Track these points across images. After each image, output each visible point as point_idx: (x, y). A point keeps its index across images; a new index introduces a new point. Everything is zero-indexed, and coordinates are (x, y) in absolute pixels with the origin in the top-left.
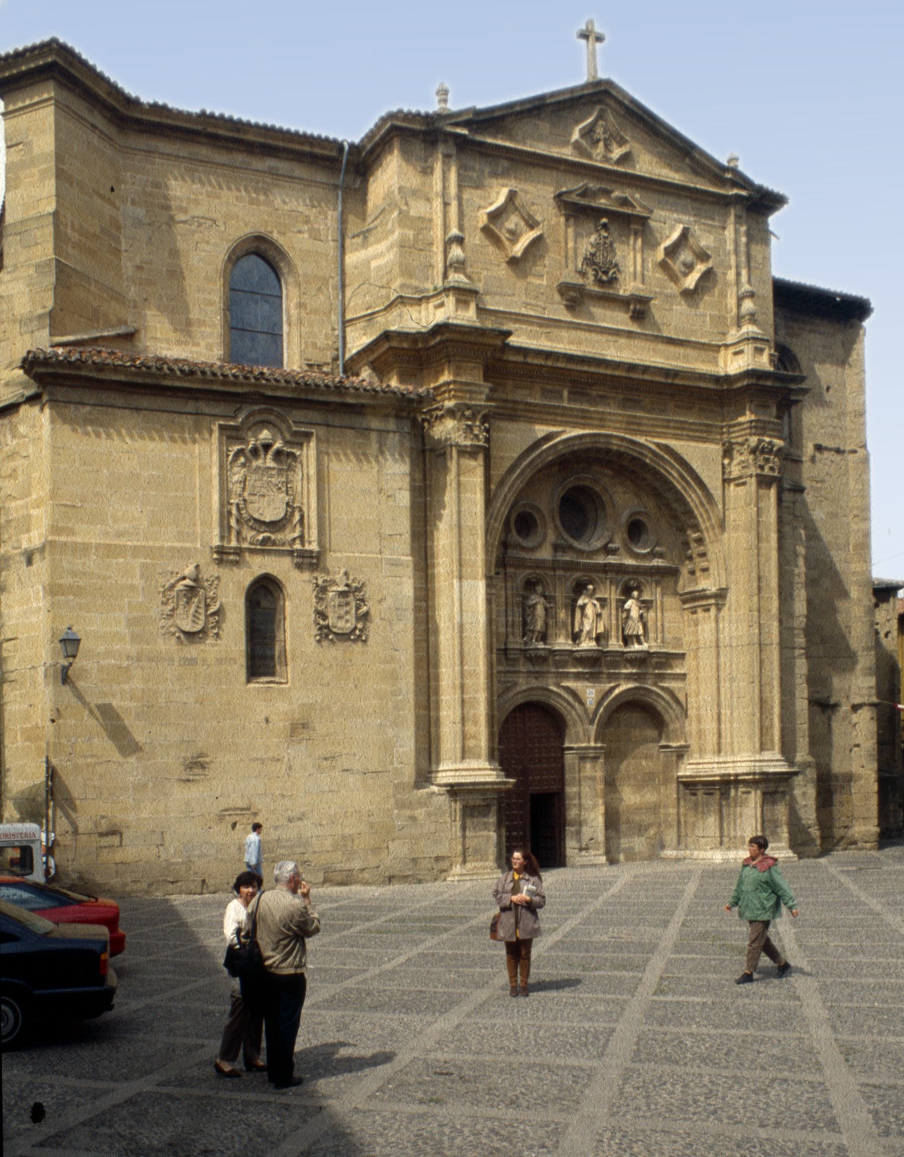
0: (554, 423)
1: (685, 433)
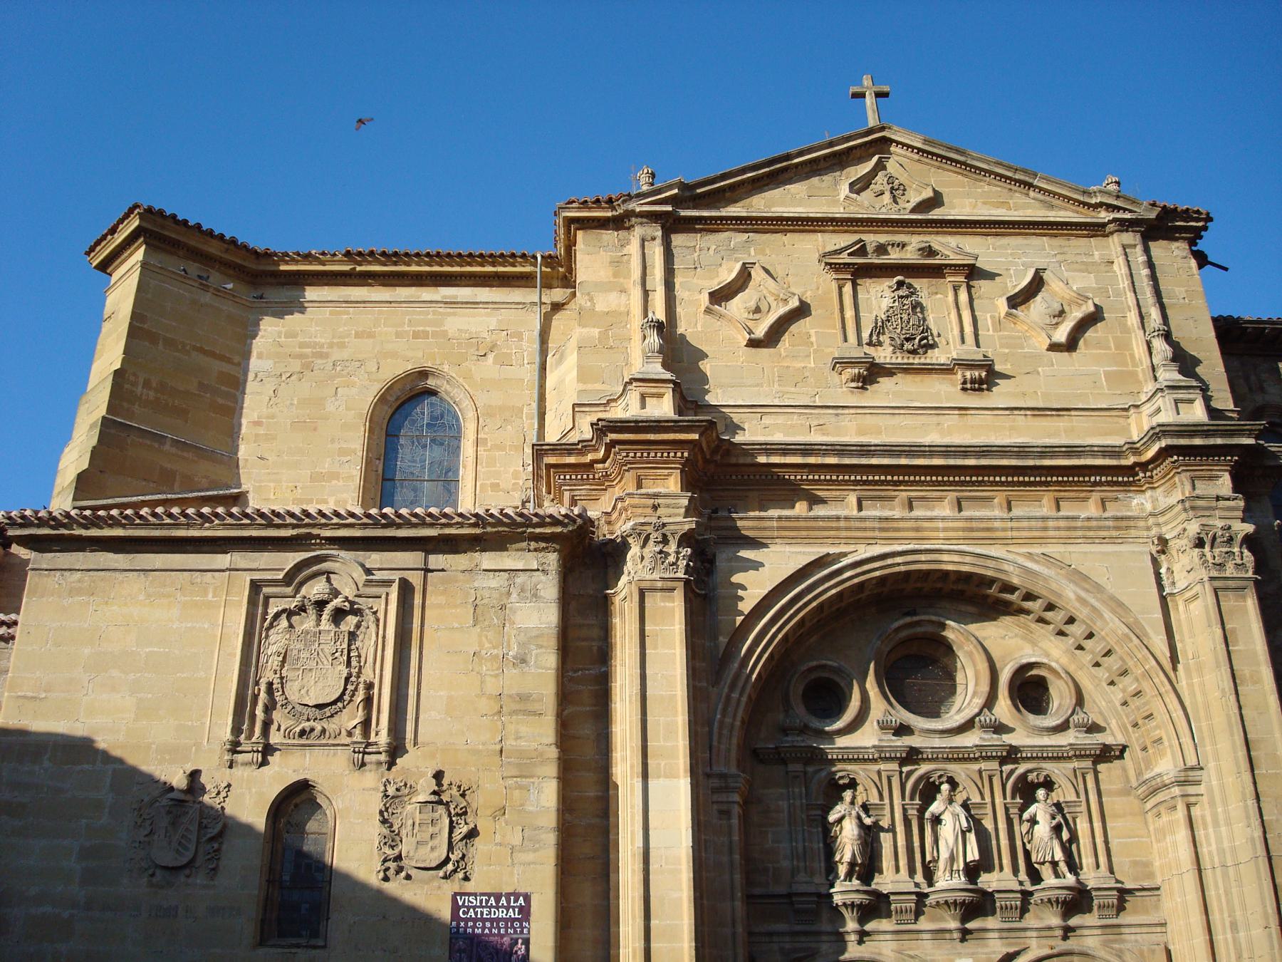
0: (836, 540)
1: (1080, 533)
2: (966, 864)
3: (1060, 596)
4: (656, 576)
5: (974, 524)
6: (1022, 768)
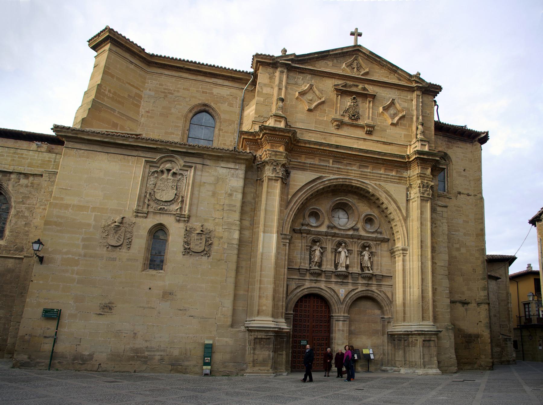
1: (389, 180)
2: (346, 265)
3: (381, 196)
4: (273, 175)
6: (363, 242)
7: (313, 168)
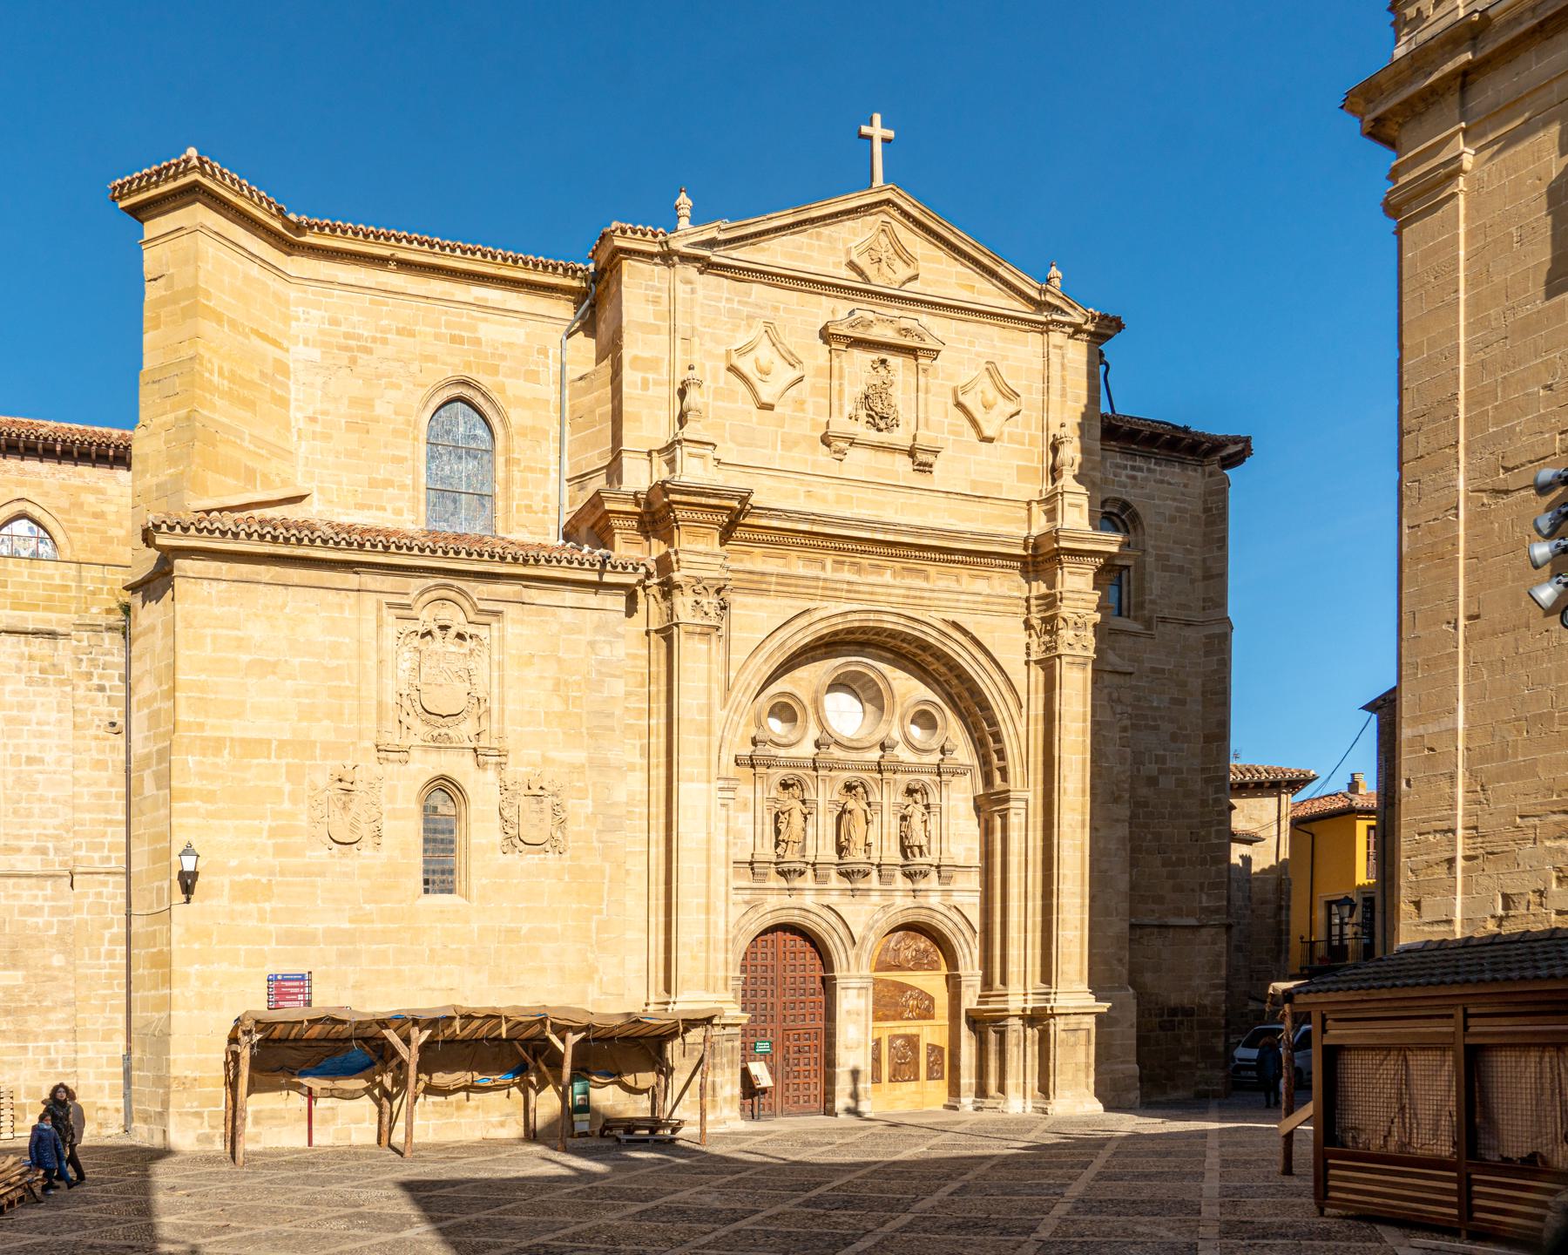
0: (812, 599)
5: (912, 593)
7: (787, 585)
